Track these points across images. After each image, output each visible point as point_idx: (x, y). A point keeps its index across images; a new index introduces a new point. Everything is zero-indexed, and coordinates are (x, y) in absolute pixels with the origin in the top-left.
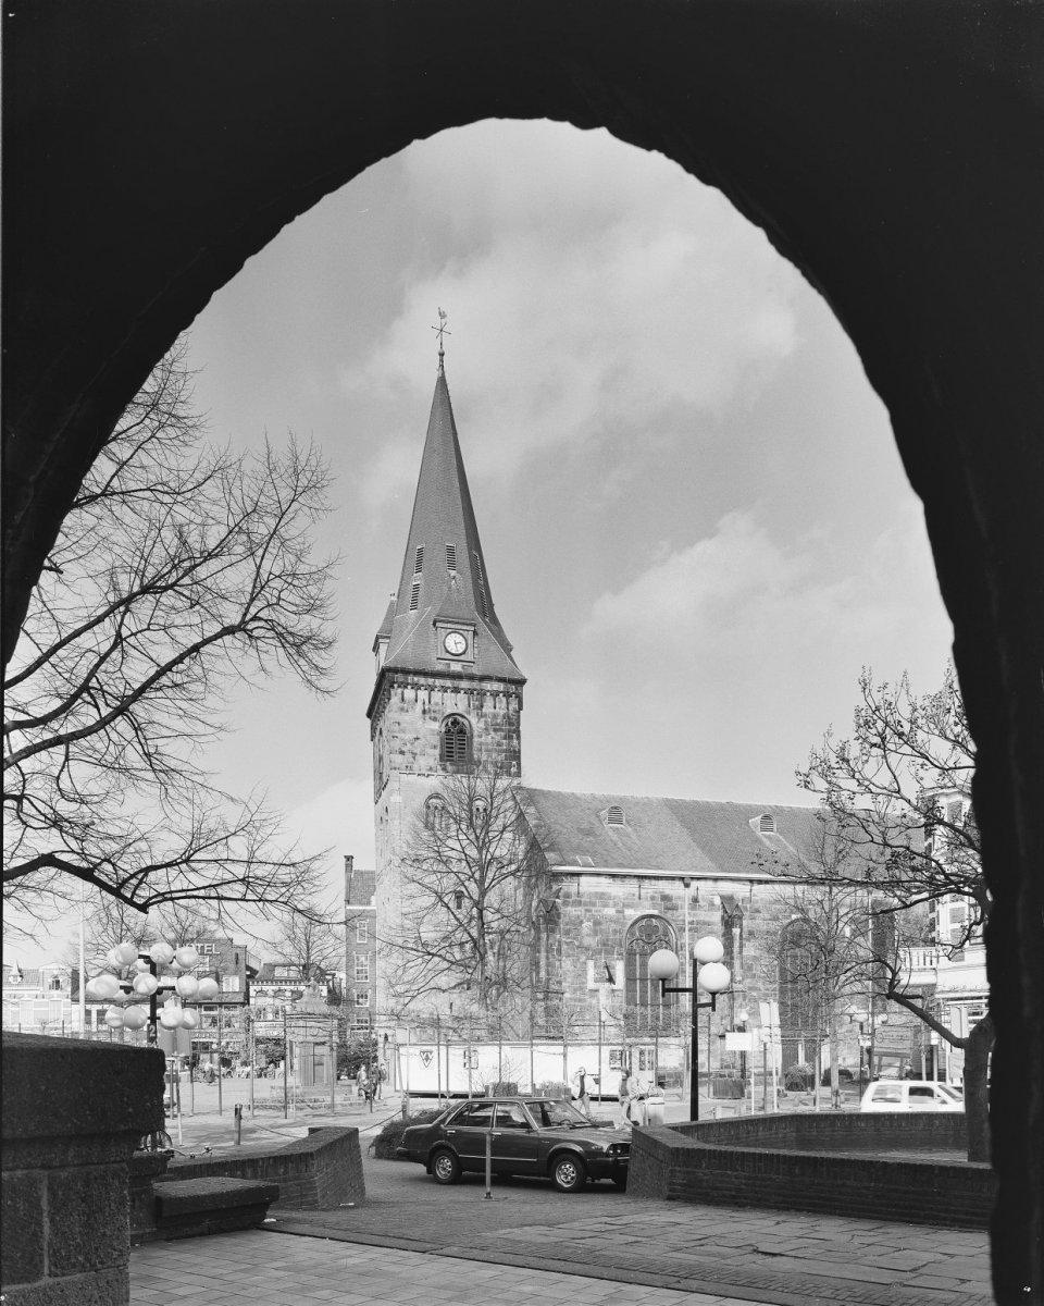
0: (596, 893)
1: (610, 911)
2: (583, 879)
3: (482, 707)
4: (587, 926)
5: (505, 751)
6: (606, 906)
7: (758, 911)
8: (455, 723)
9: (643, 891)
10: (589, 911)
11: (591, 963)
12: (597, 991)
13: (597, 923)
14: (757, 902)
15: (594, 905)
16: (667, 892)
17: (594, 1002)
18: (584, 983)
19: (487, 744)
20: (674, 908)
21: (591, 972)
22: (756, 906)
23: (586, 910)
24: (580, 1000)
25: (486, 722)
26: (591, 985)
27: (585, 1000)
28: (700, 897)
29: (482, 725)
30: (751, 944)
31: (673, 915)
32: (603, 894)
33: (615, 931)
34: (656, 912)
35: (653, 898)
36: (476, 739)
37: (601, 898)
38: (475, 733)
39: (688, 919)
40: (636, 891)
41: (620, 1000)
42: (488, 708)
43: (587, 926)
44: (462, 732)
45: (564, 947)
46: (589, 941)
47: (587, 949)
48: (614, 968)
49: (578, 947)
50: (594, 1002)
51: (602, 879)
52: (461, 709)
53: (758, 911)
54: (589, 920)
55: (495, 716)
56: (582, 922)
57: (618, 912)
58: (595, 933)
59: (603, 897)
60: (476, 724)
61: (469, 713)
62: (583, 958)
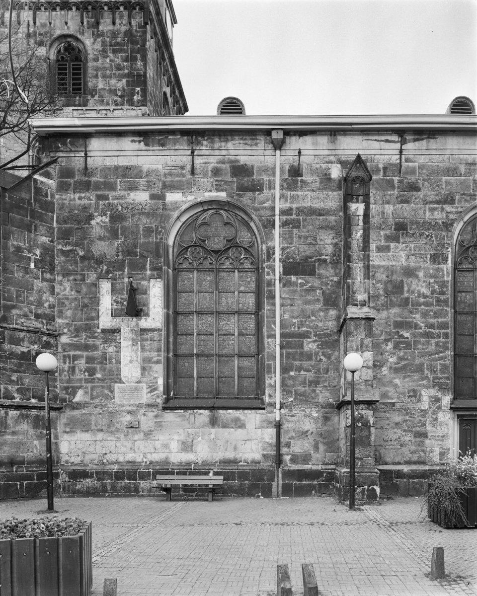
0: (117, 168)
1: (141, 197)
2: (95, 144)
3: (98, 23)
4: (99, 221)
5: (126, 76)
6: (133, 188)
7: (414, 188)
8: (69, 48)
9: (198, 161)
10: (106, 198)
11: (105, 286)
12: (116, 331)
13: (117, 218)
14: (413, 171)
15: (112, 187)
16: (243, 160)
17: (111, 349)
18: (92, 319)
19: (105, 69)
20: (257, 187)
21: (106, 302)
22: (412, 178)
23: (99, 197)
24: (86, 347)
25: (103, 42)
26: (106, 321)
27: (95, 348)
28: (305, 166)
29: (98, 46)
30: (401, 246)
31: (253, 200)
32: (128, 168)
33: (148, 231)
34: (222, 196)
35: (216, 172)
36: (91, 64)
37: (124, 176)
38: (91, 56)
39: (279, 205)
40: (186, 160)
41: (156, 345)
42: (105, 25)
43: (99, 221)
44: (78, 59)
45: (59, 260)
46: (101, 248)
47: (99, 262)
48: (145, 292)
49: (83, 258)
50: (111, 349)
51: (127, 144)
52: (72, 28)
53: (414, 188)
54: (103, 213)
55: (114, 34)
56: (91, 217)
57: (153, 197)
58: (113, 234)
59: (129, 175)
60: (90, 44)
61: (83, 33)
62: (92, 277)
